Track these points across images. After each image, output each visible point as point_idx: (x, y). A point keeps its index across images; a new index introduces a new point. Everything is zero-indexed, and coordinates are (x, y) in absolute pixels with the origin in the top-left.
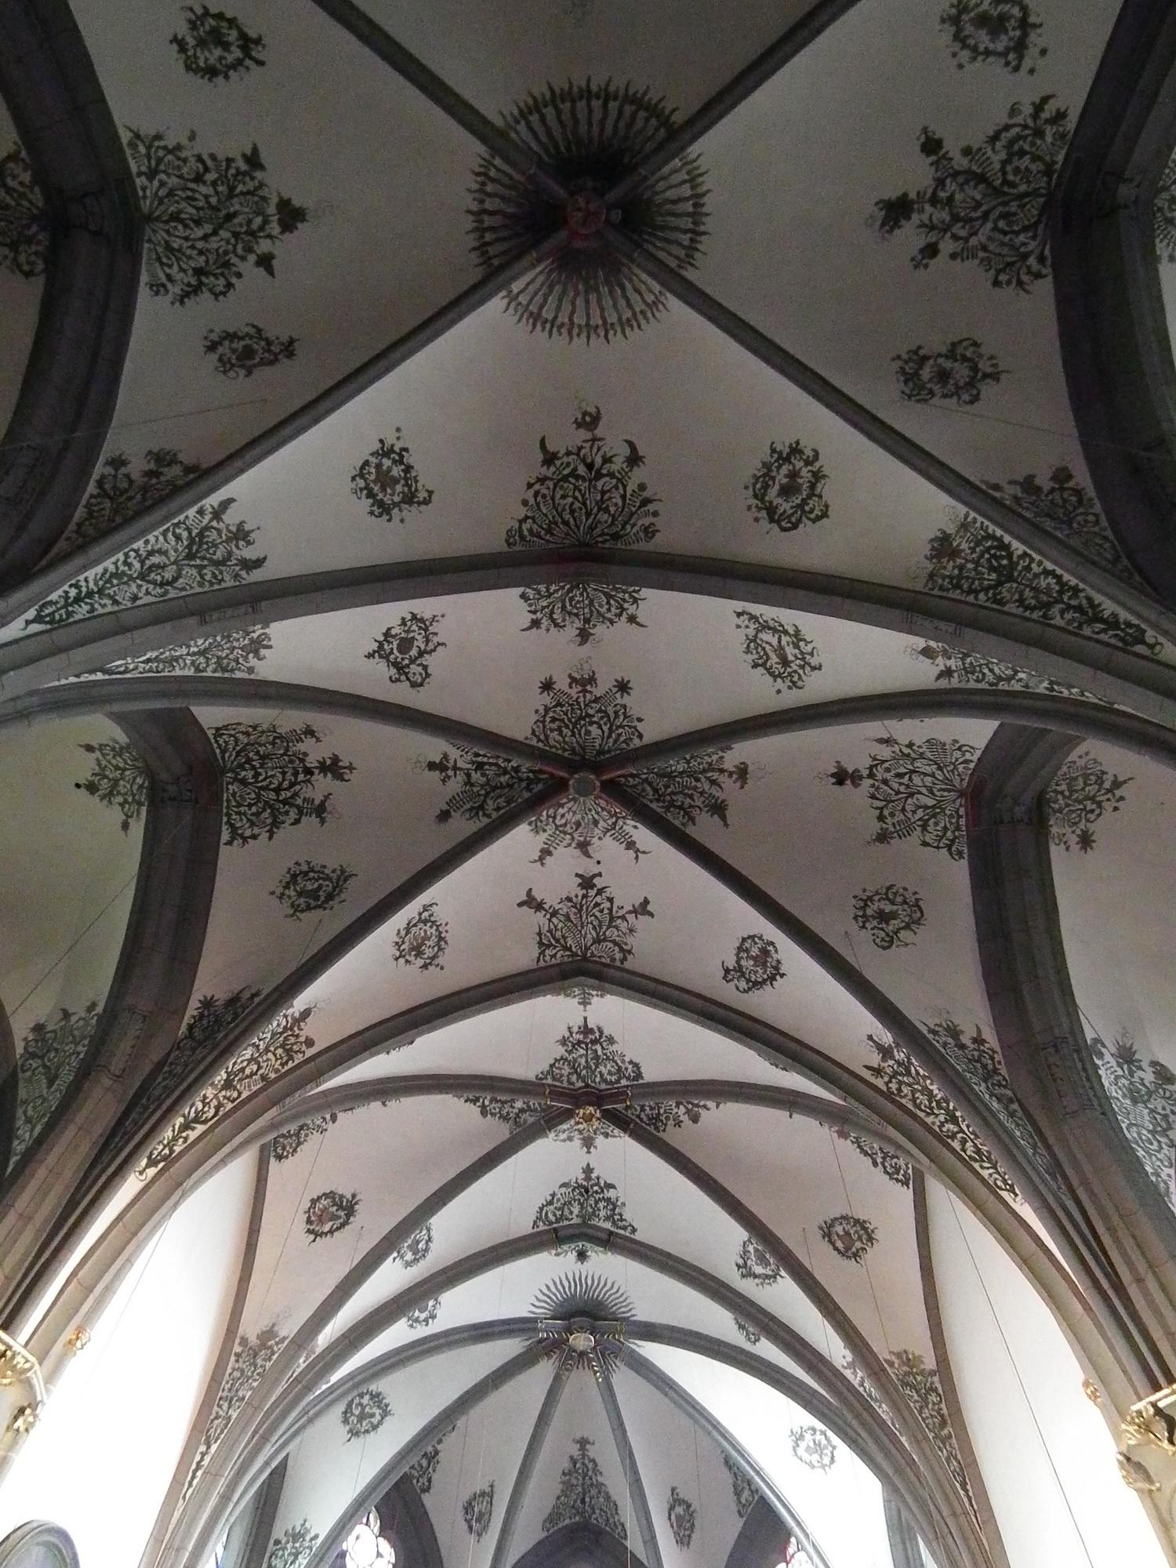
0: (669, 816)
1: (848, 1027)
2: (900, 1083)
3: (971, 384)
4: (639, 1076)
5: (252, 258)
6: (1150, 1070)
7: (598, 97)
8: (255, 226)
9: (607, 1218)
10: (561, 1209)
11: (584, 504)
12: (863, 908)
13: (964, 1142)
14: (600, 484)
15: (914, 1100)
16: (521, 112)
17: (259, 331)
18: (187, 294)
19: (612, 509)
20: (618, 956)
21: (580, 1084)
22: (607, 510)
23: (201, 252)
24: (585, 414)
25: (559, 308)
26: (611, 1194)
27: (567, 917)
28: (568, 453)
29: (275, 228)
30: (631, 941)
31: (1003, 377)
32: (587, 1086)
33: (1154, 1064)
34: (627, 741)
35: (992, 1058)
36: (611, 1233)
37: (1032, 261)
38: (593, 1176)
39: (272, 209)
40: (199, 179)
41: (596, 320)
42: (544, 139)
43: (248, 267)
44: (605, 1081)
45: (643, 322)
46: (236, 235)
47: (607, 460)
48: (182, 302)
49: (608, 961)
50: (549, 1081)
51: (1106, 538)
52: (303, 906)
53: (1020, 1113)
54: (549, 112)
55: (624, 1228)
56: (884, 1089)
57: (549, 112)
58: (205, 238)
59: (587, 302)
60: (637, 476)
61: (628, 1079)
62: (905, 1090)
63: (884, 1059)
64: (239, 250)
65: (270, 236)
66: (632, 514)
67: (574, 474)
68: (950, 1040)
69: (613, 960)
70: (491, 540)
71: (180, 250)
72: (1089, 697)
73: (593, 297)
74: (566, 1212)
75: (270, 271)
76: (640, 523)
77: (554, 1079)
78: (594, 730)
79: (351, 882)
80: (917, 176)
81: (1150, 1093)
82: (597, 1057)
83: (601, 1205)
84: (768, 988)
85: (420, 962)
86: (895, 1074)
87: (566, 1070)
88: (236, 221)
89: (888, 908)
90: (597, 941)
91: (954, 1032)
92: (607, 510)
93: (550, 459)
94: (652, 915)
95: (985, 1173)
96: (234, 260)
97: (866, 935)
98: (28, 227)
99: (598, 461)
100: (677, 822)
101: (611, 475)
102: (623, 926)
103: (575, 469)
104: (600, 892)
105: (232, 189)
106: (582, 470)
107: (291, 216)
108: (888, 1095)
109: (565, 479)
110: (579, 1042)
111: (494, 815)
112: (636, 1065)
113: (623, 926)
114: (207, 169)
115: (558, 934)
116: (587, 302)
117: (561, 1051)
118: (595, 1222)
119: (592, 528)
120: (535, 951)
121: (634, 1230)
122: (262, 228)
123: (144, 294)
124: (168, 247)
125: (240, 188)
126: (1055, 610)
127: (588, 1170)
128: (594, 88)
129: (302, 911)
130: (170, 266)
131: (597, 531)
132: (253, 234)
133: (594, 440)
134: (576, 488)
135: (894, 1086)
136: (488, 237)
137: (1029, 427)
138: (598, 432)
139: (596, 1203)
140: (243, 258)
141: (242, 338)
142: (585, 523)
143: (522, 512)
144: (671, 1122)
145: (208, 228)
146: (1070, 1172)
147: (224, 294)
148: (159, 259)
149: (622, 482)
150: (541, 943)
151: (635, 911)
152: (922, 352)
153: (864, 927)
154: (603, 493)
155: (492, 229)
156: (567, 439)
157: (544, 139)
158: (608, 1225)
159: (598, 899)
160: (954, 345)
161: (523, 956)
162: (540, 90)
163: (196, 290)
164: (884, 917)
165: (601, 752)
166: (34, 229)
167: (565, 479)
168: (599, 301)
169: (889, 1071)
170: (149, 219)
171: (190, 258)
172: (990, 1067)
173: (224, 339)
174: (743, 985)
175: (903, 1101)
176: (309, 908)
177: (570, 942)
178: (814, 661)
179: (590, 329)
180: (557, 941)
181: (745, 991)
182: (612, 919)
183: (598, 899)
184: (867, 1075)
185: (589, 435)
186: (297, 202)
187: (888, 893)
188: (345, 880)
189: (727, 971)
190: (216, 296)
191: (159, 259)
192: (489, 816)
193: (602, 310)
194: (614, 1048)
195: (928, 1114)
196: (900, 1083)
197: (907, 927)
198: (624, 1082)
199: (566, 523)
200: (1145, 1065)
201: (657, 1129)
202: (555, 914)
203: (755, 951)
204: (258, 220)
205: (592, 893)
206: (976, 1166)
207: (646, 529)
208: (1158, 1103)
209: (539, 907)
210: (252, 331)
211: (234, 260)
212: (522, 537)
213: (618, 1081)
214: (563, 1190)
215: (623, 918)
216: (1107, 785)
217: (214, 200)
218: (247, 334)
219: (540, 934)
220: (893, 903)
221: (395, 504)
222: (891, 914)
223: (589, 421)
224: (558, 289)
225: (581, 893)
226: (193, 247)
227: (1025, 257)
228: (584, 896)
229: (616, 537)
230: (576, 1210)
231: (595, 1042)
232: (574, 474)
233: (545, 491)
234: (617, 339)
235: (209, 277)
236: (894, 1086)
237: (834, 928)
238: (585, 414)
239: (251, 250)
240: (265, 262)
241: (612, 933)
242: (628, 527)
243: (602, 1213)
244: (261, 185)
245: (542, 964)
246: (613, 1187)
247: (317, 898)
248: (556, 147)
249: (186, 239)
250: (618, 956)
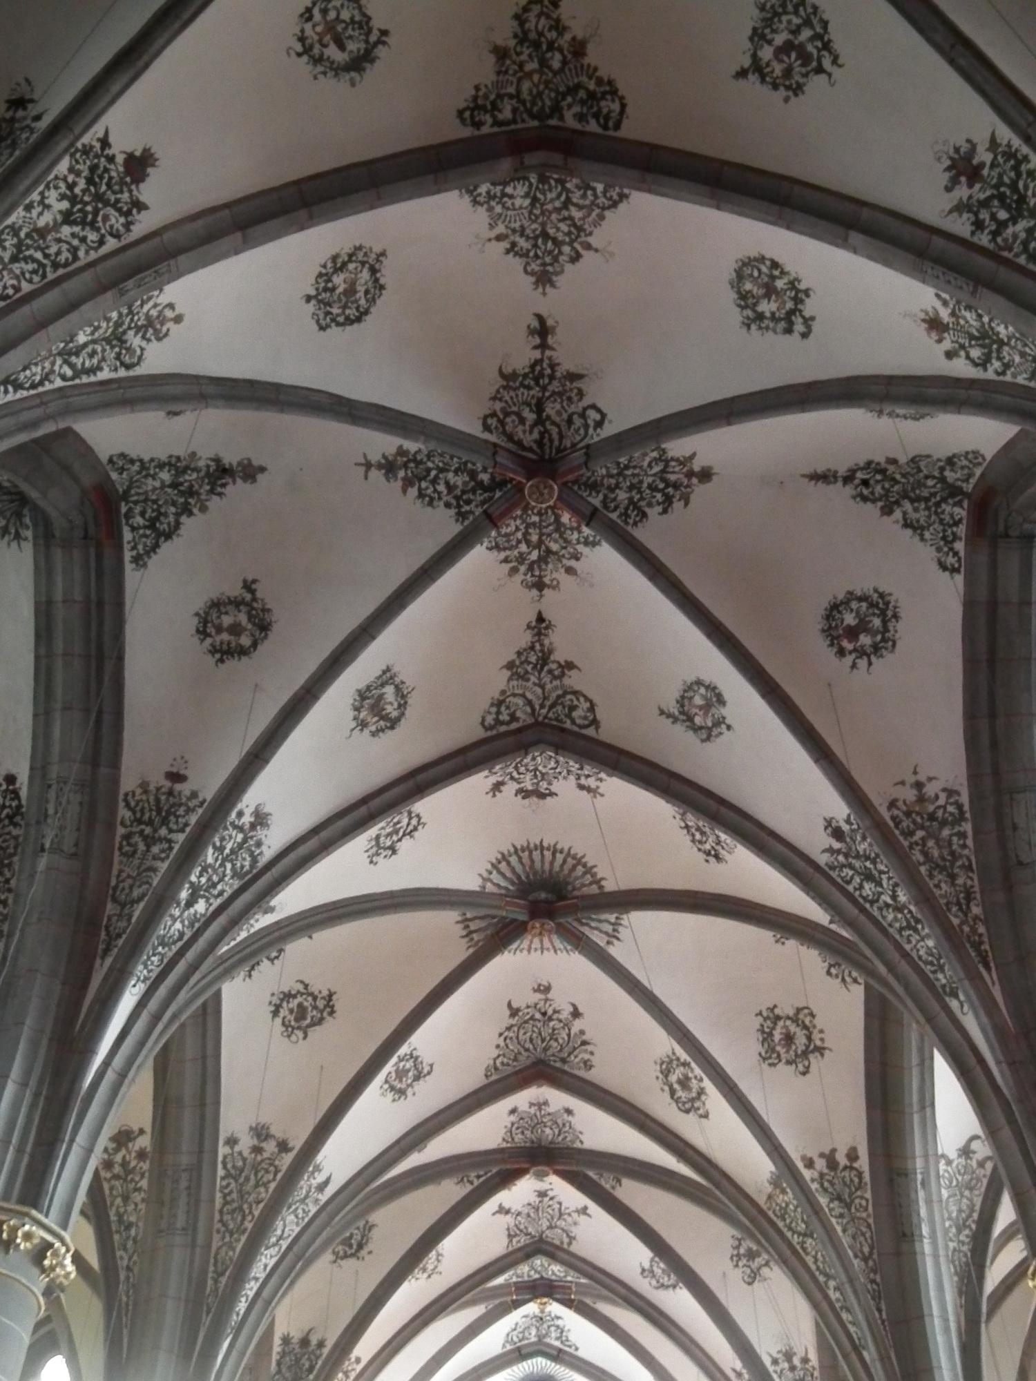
0: (603, 1183)
3: (805, 1054)
7: (548, 849)
9: (557, 1339)
10: (523, 1332)
11: (540, 1034)
14: (551, 1024)
16: (493, 865)
17: (306, 986)
19: (561, 1041)
20: (566, 1240)
21: (537, 1276)
22: (556, 1040)
26: (559, 1322)
27: (528, 1215)
28: (528, 1007)
30: (575, 1231)
31: (827, 1053)
32: (542, 1278)
34: (573, 1142)
36: (560, 1350)
42: (509, 874)
44: (553, 1273)
51: (869, 1226)
52: (341, 1253)
55: (570, 1346)
60: (577, 1025)
66: (575, 1049)
67: (532, 1018)
69: (562, 1243)
70: (474, 1079)
74: (527, 1334)
76: (580, 1056)
77: (518, 1276)
78: (548, 1131)
79: (375, 1232)
85: (425, 1275)
90: (550, 1227)
92: (556, 1040)
93: (514, 1012)
94: (589, 1216)
99: (550, 1012)
100: (608, 1187)
101: (560, 1021)
102: (569, 1219)
104: (552, 1199)
106: (538, 1016)
109: (526, 1022)
111: (476, 1183)
113: (569, 1219)
115: (522, 1227)
118: (547, 1340)
119: (545, 1050)
120: (505, 1241)
121: (577, 1349)
128: (545, 844)
129: (342, 1258)
131: (549, 1053)
133: (546, 1000)
138: (549, 996)
141: (295, 996)
142: (541, 1045)
143: (496, 1052)
149: (567, 1025)
150: (509, 1236)
151: (577, 1211)
152: (777, 1011)
153: (737, 1266)
157: (509, 874)
158: (557, 1344)
160: (799, 1010)
162: (506, 848)
165: (551, 1142)
167: (526, 1022)
173: (282, 1000)
174: (654, 1282)
176: (346, 1256)
177: (530, 1230)
181: (657, 1288)
182: (561, 1214)
188: (370, 1230)
192: (472, 1183)
199: (527, 1050)
202: (519, 1214)
207: (585, 1062)
209: (508, 1212)
210: (301, 987)
212: (496, 1069)
215: (569, 1215)
218: (298, 992)
219: (508, 1229)
221: (409, 1086)
225: (538, 1200)
229: (564, 1061)
230: (534, 1331)
232: (532, 1018)
233: (511, 1034)
241: (561, 1223)
242: (572, 1057)
243: (553, 1335)
245: (510, 1249)
247: (351, 1246)
248: (519, 877)
250: (566, 1240)
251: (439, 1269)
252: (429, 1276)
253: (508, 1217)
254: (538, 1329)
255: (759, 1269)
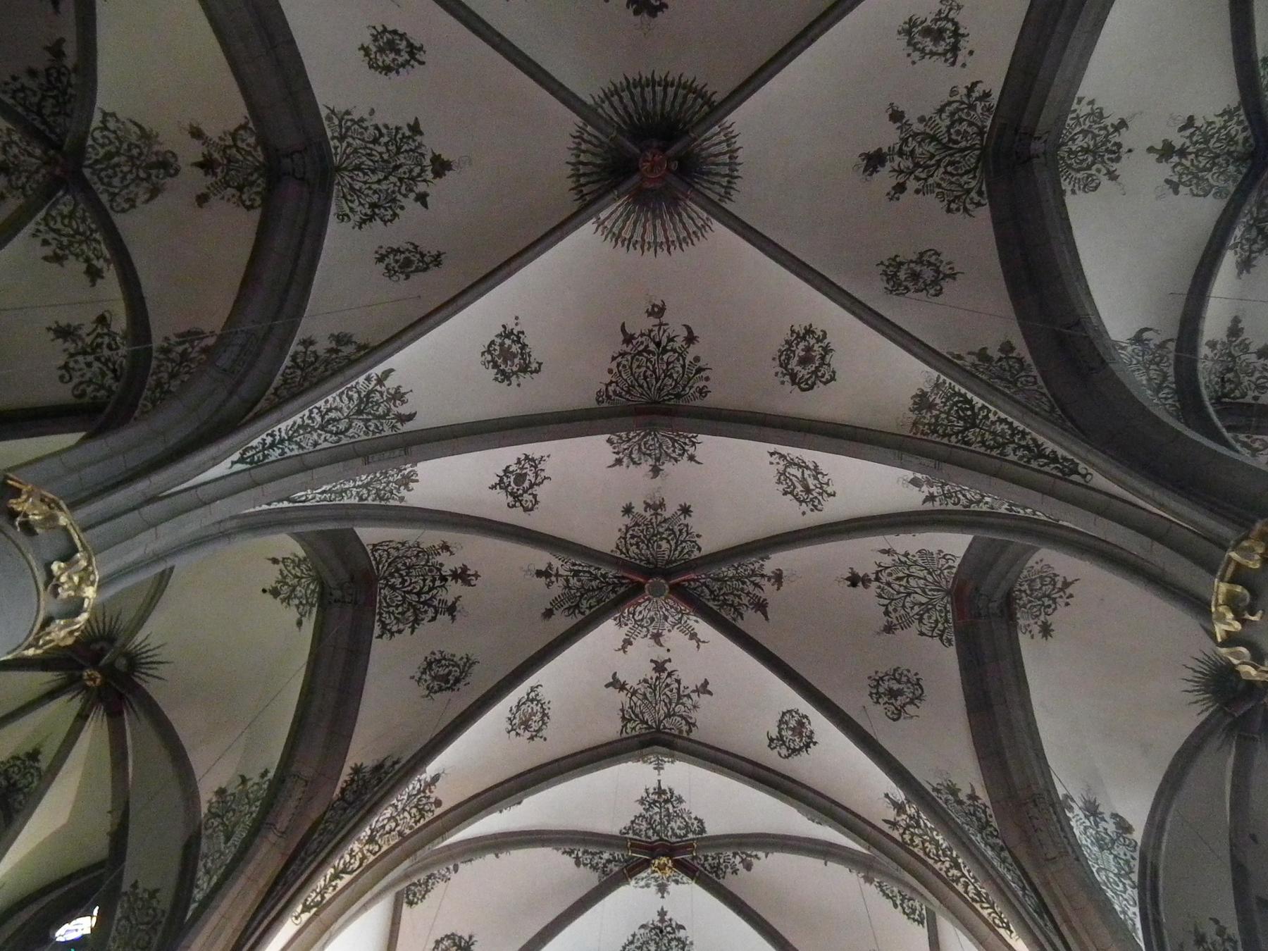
0: (724, 614)
1: (871, 789)
2: (913, 834)
4: (703, 830)
5: (412, 196)
6: (1111, 821)
8: (414, 174)
11: (654, 372)
12: (877, 686)
13: (966, 885)
14: (665, 357)
15: (924, 849)
17: (416, 247)
18: (364, 221)
19: (675, 376)
21: (655, 838)
22: (671, 376)
23: (375, 192)
24: (654, 306)
25: (634, 230)
26: (681, 934)
28: (642, 335)
29: (429, 175)
30: (695, 716)
32: (661, 839)
33: (1115, 816)
35: (985, 812)
37: (973, 194)
38: (667, 918)
39: (427, 162)
40: (375, 141)
41: (661, 239)
42: (621, 112)
43: (409, 203)
44: (675, 834)
45: (695, 240)
46: (401, 180)
47: (671, 340)
48: (360, 227)
49: (677, 733)
50: (631, 835)
51: (1043, 394)
53: (1010, 860)
54: (625, 94)
56: (900, 839)
57: (625, 94)
58: (379, 182)
59: (655, 227)
60: (693, 351)
61: (694, 833)
62: (917, 840)
63: (898, 814)
64: (403, 191)
65: (425, 181)
66: (690, 379)
67: (646, 350)
68: (950, 797)
69: (681, 731)
70: (584, 399)
71: (360, 190)
72: (1040, 516)
73: (658, 222)
75: (425, 205)
77: (635, 833)
78: (664, 544)
80: (888, 137)
81: (1113, 841)
82: (668, 815)
83: (674, 943)
84: (804, 754)
86: (908, 827)
87: (644, 826)
88: (401, 170)
89: (896, 686)
90: (668, 715)
91: (953, 791)
92: (671, 376)
93: (628, 339)
94: (710, 693)
95: (985, 913)
96: (399, 197)
97: (880, 708)
98: (252, 174)
99: (664, 340)
101: (674, 351)
102: (688, 702)
103: (647, 346)
105: (399, 148)
106: (652, 347)
107: (441, 167)
108: (903, 845)
109: (640, 353)
110: (655, 802)
111: (588, 612)
112: (700, 821)
113: (688, 702)
114: (381, 135)
115: (637, 710)
116: (655, 227)
117: (640, 809)
119: (660, 390)
122: (419, 175)
123: (332, 221)
124: (352, 188)
125: (405, 147)
126: (1009, 449)
127: (662, 913)
130: (352, 202)
132: (413, 179)
134: (648, 360)
135: (907, 837)
136: (582, 180)
137: (980, 313)
138: (664, 320)
139: (669, 941)
140: (405, 196)
143: (608, 378)
144: (729, 870)
145: (381, 175)
146: (1054, 912)
147: (391, 221)
148: (344, 197)
150: (623, 718)
151: (697, 691)
153: (877, 702)
154: (668, 363)
155: (584, 175)
156: (640, 324)
159: (669, 681)
161: (610, 729)
163: (371, 218)
164: (893, 694)
165: (669, 562)
166: (256, 175)
167: (640, 353)
168: (663, 225)
169: (903, 824)
170: (338, 169)
171: (367, 195)
172: (984, 820)
174: (784, 752)
175: (916, 850)
178: (830, 490)
179: (657, 245)
180: (637, 716)
181: (786, 757)
182: (680, 697)
183: (669, 681)
184: (886, 828)
185: (657, 321)
186: (445, 157)
187: (896, 675)
189: (771, 740)
190: (385, 222)
191: (344, 197)
192: (583, 613)
193: (665, 231)
194: (683, 806)
195: (936, 862)
196: (913, 834)
197: (912, 702)
198: (691, 836)
199: (641, 386)
200: (1107, 818)
201: (717, 876)
202: (634, 693)
203: (793, 723)
204: (417, 170)
205: (664, 675)
206: (977, 906)
208: (1120, 850)
210: (411, 248)
211: (399, 197)
212: (609, 397)
213: (685, 835)
214: (642, 931)
216: (1059, 585)
217: (386, 156)
219: (622, 710)
220: (899, 682)
221: (514, 373)
222: (898, 691)
223: (657, 311)
224: (633, 216)
225: (655, 675)
226: (370, 188)
227: (968, 191)
228: (658, 678)
229: (678, 396)
231: (667, 801)
232: (646, 350)
234: (676, 252)
235: (381, 210)
236: (907, 837)
237: (854, 702)
238: (654, 306)
239: (411, 190)
240: (422, 198)
241: (679, 709)
244: (420, 145)
245: (624, 735)
246: (682, 927)
249: (365, 183)
250: (685, 728)
251: (543, 733)
252: (532, 738)
253: (623, 693)
254: (657, 943)
255: (903, 706)
